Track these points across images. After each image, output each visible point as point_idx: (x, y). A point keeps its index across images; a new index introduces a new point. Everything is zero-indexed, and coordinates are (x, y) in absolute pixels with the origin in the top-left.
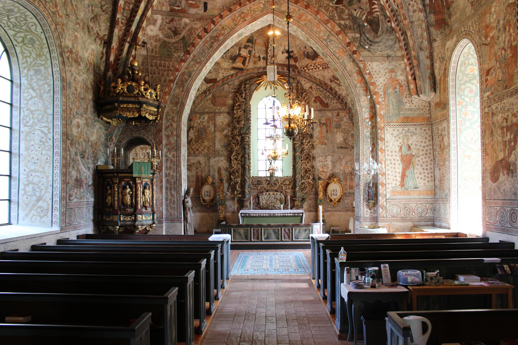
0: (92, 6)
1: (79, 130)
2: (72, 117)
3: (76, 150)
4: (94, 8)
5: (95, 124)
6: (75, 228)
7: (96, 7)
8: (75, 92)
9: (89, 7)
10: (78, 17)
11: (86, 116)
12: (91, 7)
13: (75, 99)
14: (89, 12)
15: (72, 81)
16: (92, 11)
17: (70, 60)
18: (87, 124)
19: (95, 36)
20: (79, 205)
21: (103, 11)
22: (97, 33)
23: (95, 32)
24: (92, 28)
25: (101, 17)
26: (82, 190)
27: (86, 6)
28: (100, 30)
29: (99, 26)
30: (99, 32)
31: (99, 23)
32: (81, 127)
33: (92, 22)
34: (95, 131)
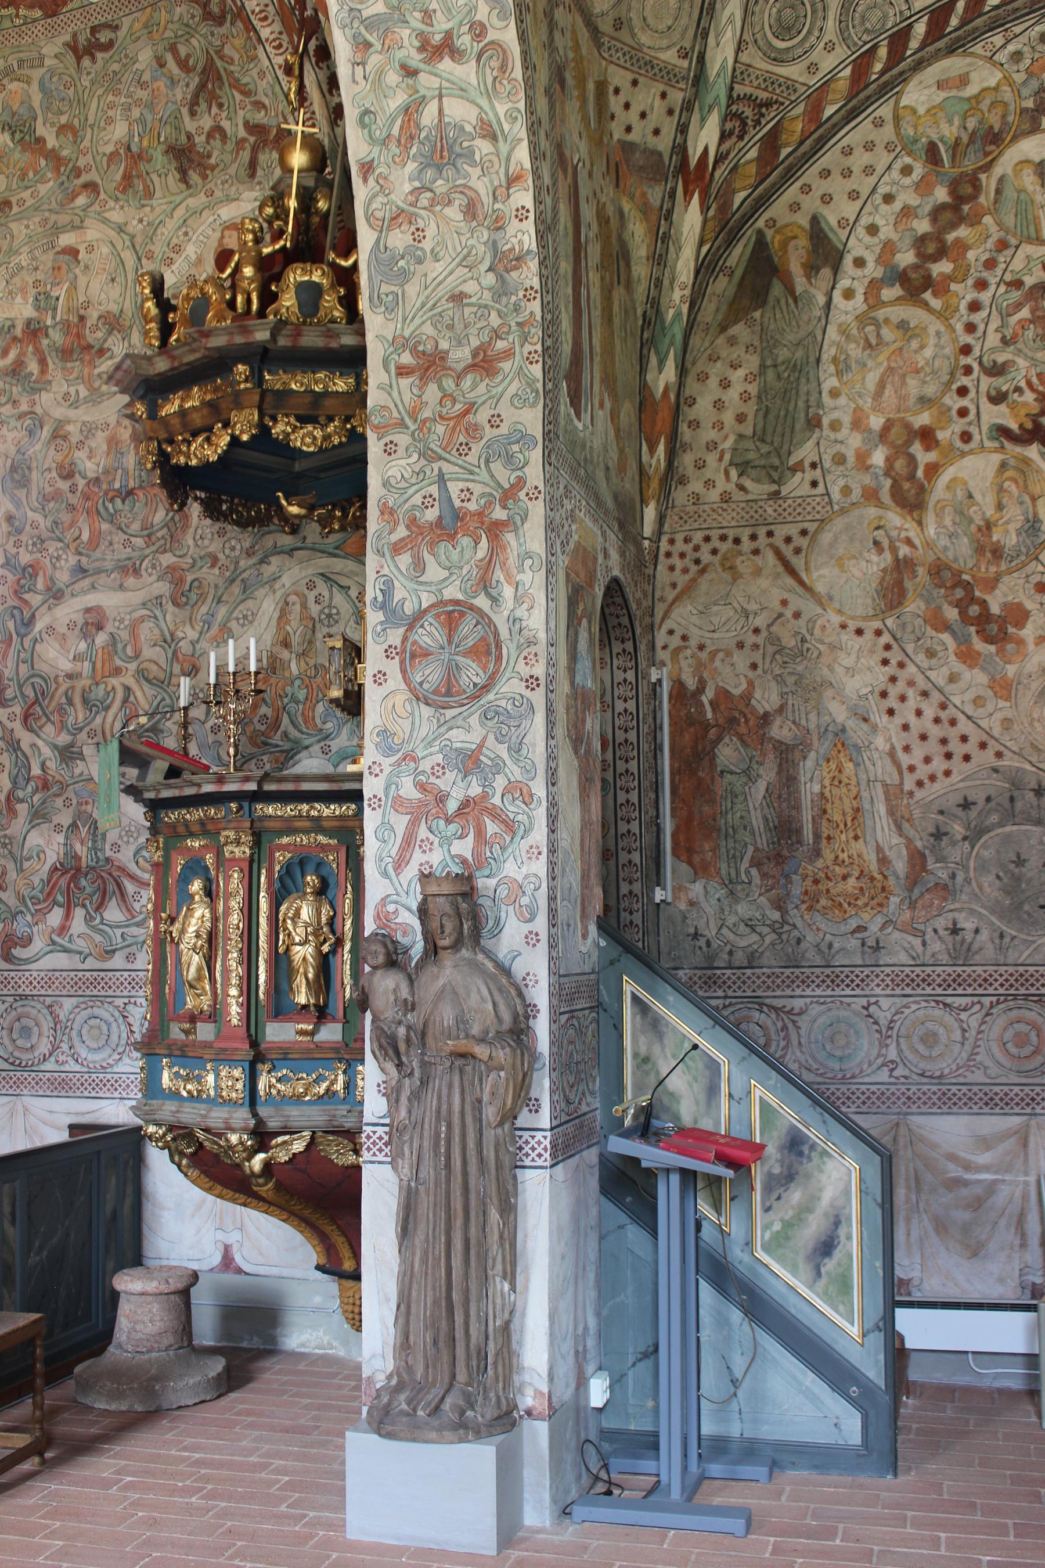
0: (173, 49)
1: (101, 639)
2: (35, 600)
3: (64, 739)
4: (183, 51)
5: (268, 570)
6: (62, 1087)
7: (189, 31)
8: (64, 485)
9: (162, 65)
10: (81, 163)
11: (167, 559)
12: (169, 58)
13: (66, 517)
14: (173, 82)
15: (36, 448)
16: (184, 65)
17: (33, 367)
18: (183, 593)
19: (246, 155)
20: (94, 983)
21: (220, 20)
22: (252, 128)
23: (242, 133)
24: (217, 130)
25: (228, 50)
26: (113, 913)
27: (146, 77)
28: (259, 105)
29: (247, 93)
30: (260, 117)
31: (236, 84)
32: (109, 628)
33: (203, 106)
34: (268, 606)
